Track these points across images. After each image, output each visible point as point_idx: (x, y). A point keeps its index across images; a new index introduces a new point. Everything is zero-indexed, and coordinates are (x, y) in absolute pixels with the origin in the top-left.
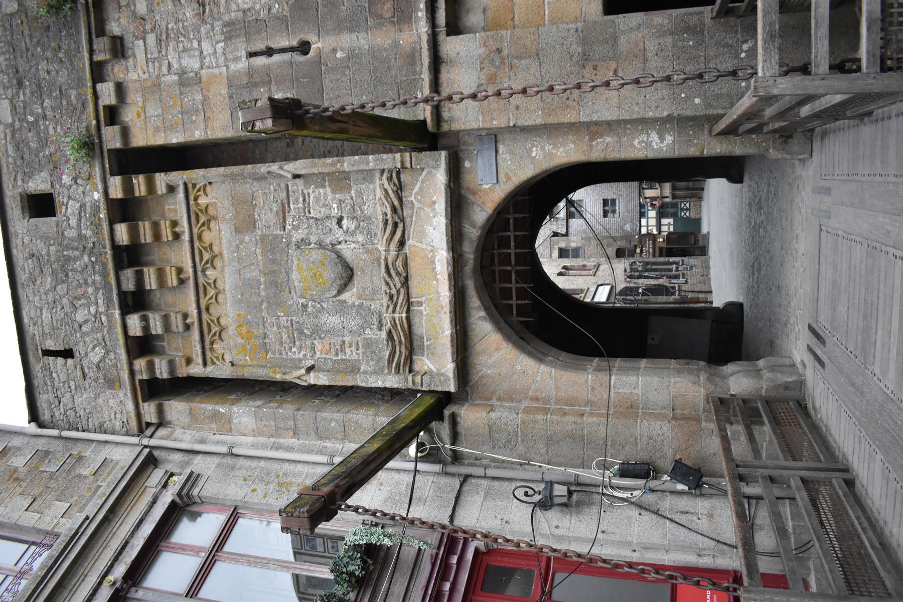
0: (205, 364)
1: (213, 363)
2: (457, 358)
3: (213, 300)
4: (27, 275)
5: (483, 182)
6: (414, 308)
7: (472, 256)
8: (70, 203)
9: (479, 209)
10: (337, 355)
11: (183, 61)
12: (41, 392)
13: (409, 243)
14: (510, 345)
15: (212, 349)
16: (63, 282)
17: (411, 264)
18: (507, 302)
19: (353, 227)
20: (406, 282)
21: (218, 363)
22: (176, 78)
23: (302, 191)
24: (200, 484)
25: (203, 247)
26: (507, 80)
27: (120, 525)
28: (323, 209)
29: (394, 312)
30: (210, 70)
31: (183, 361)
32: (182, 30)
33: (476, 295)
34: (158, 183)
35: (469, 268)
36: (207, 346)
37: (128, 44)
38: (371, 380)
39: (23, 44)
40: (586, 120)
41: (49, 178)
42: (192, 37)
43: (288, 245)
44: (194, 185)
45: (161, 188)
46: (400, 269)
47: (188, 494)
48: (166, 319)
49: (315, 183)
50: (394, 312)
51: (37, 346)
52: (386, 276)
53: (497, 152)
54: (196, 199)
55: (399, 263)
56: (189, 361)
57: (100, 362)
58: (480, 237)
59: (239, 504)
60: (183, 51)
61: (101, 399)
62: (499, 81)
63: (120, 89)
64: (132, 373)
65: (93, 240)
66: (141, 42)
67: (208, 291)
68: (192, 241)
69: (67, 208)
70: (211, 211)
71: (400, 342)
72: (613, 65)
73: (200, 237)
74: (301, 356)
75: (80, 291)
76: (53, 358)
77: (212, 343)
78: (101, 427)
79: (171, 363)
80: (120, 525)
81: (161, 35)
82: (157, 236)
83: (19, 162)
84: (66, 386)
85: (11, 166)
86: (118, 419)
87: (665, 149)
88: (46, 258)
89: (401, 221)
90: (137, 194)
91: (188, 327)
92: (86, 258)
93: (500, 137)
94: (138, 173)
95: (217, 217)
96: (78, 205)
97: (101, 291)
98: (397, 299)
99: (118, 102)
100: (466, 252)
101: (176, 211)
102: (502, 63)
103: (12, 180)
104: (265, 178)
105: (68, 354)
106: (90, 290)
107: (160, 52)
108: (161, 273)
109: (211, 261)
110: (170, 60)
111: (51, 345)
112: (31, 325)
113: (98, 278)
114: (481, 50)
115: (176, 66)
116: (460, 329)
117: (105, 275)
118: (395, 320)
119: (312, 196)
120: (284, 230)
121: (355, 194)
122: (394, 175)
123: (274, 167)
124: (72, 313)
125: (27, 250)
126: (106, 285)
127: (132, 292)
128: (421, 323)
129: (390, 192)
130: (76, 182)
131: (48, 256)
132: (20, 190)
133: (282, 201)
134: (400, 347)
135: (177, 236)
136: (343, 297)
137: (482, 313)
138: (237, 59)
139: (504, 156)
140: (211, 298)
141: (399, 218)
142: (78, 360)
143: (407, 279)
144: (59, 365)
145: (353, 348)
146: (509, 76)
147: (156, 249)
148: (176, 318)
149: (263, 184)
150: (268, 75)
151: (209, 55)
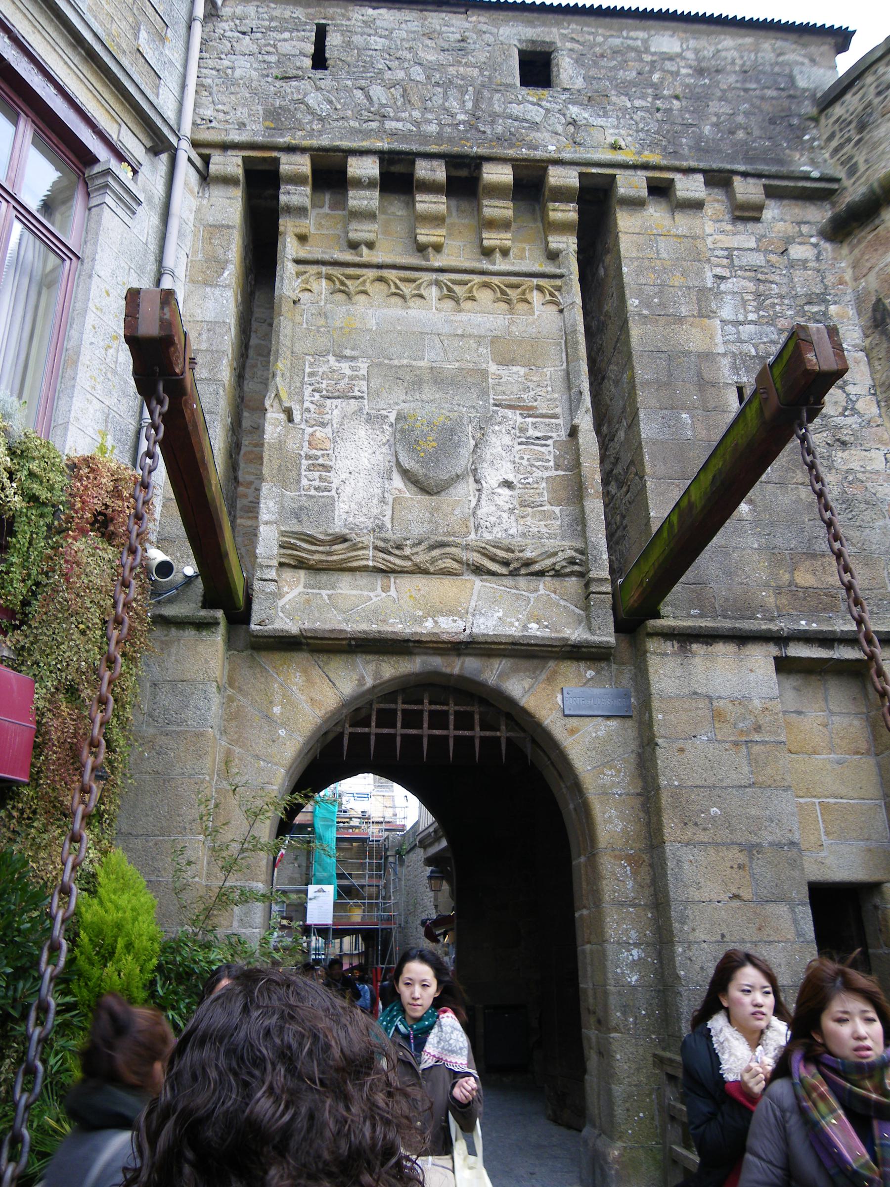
0: (298, 262)
1: (299, 274)
2: (306, 638)
3: (393, 290)
4: (438, 28)
5: (565, 694)
6: (379, 581)
7: (456, 671)
8: (541, 110)
9: (527, 686)
10: (308, 457)
11: (729, 297)
12: (260, 10)
13: (477, 583)
14: (319, 721)
15: (319, 275)
16: (428, 78)
17: (447, 581)
18: (374, 718)
19: (500, 501)
20: (421, 571)
21: (299, 280)
22: (709, 285)
23: (551, 437)
24: (119, 211)
25: (472, 287)
26: (719, 738)
27: (66, 63)
28: (525, 462)
29: (376, 548)
30: (720, 332)
31: (304, 231)
32: (768, 302)
33: (398, 674)
34: (564, 239)
35: (437, 662)
36: (324, 269)
37: (750, 226)
38: (271, 504)
39: (753, 86)
40: (668, 851)
41: (576, 87)
42: (761, 313)
43: (474, 407)
44: (559, 289)
45: (557, 242)
46: (441, 564)
47: (107, 186)
48: (370, 216)
49: (561, 456)
50: (376, 548)
51: (333, 19)
52: (432, 542)
53: (608, 717)
54: (539, 288)
55: (449, 563)
56: (302, 238)
57: (307, 105)
58: (482, 685)
59: (87, 266)
60: (743, 298)
61: (248, 95)
62: (717, 726)
63: (697, 205)
64: (291, 149)
65: (489, 131)
66: (753, 245)
67: (406, 284)
68: (483, 273)
69: (533, 104)
71: (329, 553)
72: (746, 894)
73: (486, 285)
74: (307, 404)
75: (415, 99)
76: (313, 39)
77: (329, 278)
78: (203, 86)
79: (301, 211)
80: (66, 63)
81: (762, 273)
82: (492, 224)
83: (598, 50)
84: (272, 49)
85: (591, 38)
86: (215, 114)
87: (619, 970)
88: (464, 61)
89: (511, 572)
90: (551, 205)
91: (354, 246)
92: (461, 117)
93: (629, 723)
94: (581, 212)
95: (513, 314)
96: (538, 120)
97: (414, 129)
98: (396, 555)
99: (678, 200)
100: (463, 663)
101: (521, 259)
103: (573, 35)
104: (569, 388)
105: (320, 61)
106: (416, 114)
107: (741, 268)
108: (437, 220)
109: (451, 296)
110: (730, 281)
111: (333, 40)
112: (365, 18)
113: (433, 128)
114: (757, 703)
115: (723, 287)
116: (350, 645)
118: (363, 548)
119: (543, 449)
120: (495, 405)
121: (548, 511)
122: (576, 568)
124: (382, 80)
125: (475, 36)
126: (425, 138)
127: (411, 175)
128: (356, 587)
129: (553, 560)
130: (570, 123)
131: (466, 63)
132: (559, 45)
133: (536, 408)
134: (322, 553)
135: (487, 253)
137: (369, 682)
138: (735, 369)
139: (603, 728)
140: (397, 287)
142: (310, 75)
143: (426, 572)
144: (303, 45)
145: (316, 483)
146: (724, 741)
147: (466, 221)
148: (369, 231)
149: (560, 384)
150: (715, 409)
151: (738, 333)
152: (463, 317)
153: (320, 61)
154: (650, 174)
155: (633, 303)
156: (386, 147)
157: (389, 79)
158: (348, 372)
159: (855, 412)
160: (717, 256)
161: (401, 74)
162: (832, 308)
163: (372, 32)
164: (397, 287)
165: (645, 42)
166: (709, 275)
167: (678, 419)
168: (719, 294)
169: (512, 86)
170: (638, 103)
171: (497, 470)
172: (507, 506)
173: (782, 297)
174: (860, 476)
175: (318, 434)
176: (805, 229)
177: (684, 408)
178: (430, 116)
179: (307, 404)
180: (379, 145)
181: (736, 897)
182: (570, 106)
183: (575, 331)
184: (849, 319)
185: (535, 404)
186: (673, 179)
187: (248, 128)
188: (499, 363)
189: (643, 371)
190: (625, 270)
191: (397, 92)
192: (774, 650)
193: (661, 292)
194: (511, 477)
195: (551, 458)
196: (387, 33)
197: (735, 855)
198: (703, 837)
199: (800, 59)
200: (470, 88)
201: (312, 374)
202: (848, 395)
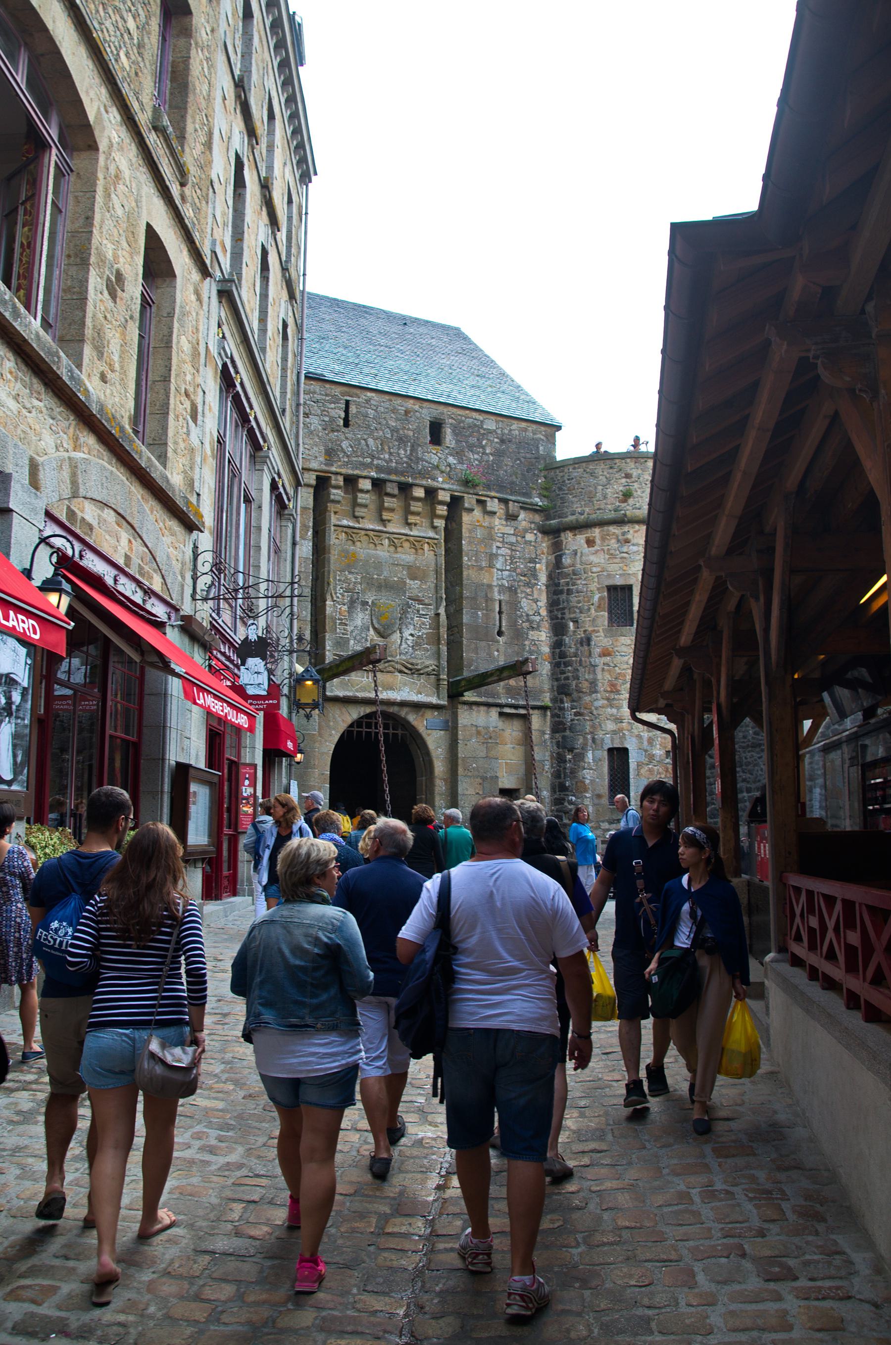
16: (392, 436)
19: (409, 642)
36: (345, 529)
54: (428, 543)
55: (391, 669)
56: (335, 513)
64: (337, 474)
66: (512, 532)
70: (420, 551)
72: (481, 793)
73: (407, 540)
77: (346, 533)
79: (338, 502)
82: (414, 513)
92: (405, 459)
111: (353, 409)
117: (396, 472)
123: (444, 604)
126: (390, 471)
135: (409, 524)
136: (371, 629)
137: (362, 714)
138: (499, 593)
149: (433, 590)
152: (398, 555)
154: (478, 497)
155: (465, 558)
156: (375, 476)
159: (539, 614)
161: (381, 433)
162: (538, 565)
165: (482, 422)
168: (496, 555)
170: (476, 456)
173: (520, 558)
176: (533, 526)
177: (480, 610)
180: (373, 474)
181: (478, 793)
183: (441, 568)
188: (411, 579)
189: (466, 593)
191: (379, 442)
192: (498, 709)
194: (413, 632)
197: (479, 780)
198: (469, 774)
199: (542, 437)
201: (339, 580)
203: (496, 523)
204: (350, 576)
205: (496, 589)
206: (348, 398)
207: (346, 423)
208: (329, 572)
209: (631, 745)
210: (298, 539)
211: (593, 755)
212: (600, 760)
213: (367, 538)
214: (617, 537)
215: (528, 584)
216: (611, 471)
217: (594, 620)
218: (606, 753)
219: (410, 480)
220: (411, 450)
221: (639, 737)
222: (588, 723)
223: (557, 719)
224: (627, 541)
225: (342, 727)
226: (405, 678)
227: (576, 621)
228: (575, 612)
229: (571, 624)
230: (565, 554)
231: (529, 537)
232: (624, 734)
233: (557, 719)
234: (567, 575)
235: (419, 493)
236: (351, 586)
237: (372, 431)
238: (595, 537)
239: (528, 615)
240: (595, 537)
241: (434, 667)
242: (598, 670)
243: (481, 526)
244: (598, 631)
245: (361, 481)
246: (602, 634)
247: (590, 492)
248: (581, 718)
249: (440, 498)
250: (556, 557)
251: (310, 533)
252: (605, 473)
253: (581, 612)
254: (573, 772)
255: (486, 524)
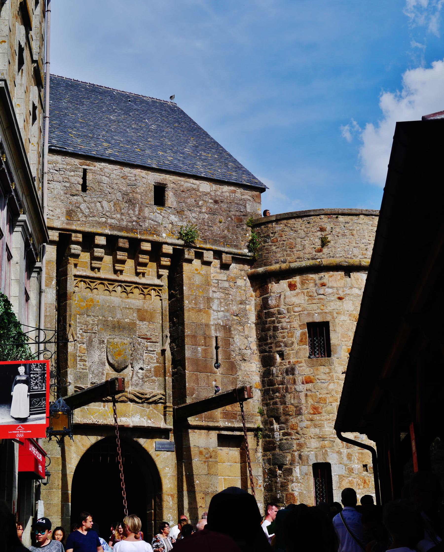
0: (75, 276)
3: (107, 288)
10: (79, 356)
13: (132, 404)
16: (123, 198)
55: (124, 398)
57: (81, 209)
66: (225, 279)
70: (148, 296)
83: (182, 189)
92: (135, 218)
102: (207, 458)
111: (89, 177)
112: (101, 167)
117: (126, 229)
119: (153, 355)
120: (138, 337)
122: (162, 401)
123: (169, 341)
132: (169, 185)
135: (137, 274)
136: (107, 364)
138: (216, 330)
140: (107, 287)
141: (144, 401)
145: (82, 367)
149: (160, 330)
152: (129, 300)
153: (84, 188)
156: (110, 233)
157: (109, 199)
158: (91, 322)
160: (214, 283)
162: (248, 306)
163: (103, 174)
164: (107, 287)
165: (198, 186)
166: (211, 291)
167: (197, 350)
169: (151, 205)
170: (194, 215)
171: (139, 364)
172: (142, 377)
173: (232, 301)
174: (249, 373)
175: (82, 347)
178: (124, 217)
179: (78, 335)
182: (171, 215)
184: (252, 311)
185: (151, 337)
186: (203, 252)
187: (61, 219)
189: (187, 332)
190: (184, 288)
191: (112, 204)
193: (196, 298)
194: (142, 366)
195: (155, 359)
196: (108, 175)
199: (249, 198)
200: (137, 205)
201: (79, 323)
202: (248, 341)
203: (212, 271)
204: (88, 319)
205: (213, 328)
206: (85, 167)
207: (84, 188)
208: (70, 316)
209: (332, 459)
210: (43, 287)
211: (300, 470)
212: (306, 474)
213: (103, 286)
214: (315, 281)
215: (240, 323)
216: (308, 225)
217: (297, 352)
218: (311, 468)
219: (139, 236)
220: (139, 211)
221: (339, 453)
222: (295, 442)
223: (268, 439)
224: (323, 285)
225: (83, 450)
226: (136, 406)
227: (282, 355)
228: (280, 346)
229: (278, 356)
230: (270, 296)
231: (240, 282)
232: (326, 451)
233: (268, 439)
234: (272, 315)
235: (147, 247)
236: (90, 327)
237: (106, 195)
238: (296, 282)
239: (240, 349)
240: (296, 282)
241: (161, 396)
242: (302, 395)
243: (199, 273)
244: (301, 362)
245: (97, 237)
246: (305, 365)
247: (291, 244)
248: (289, 437)
249: (164, 251)
250: (263, 299)
251: (54, 282)
252: (303, 227)
253: (286, 346)
254: (284, 486)
255: (203, 272)
